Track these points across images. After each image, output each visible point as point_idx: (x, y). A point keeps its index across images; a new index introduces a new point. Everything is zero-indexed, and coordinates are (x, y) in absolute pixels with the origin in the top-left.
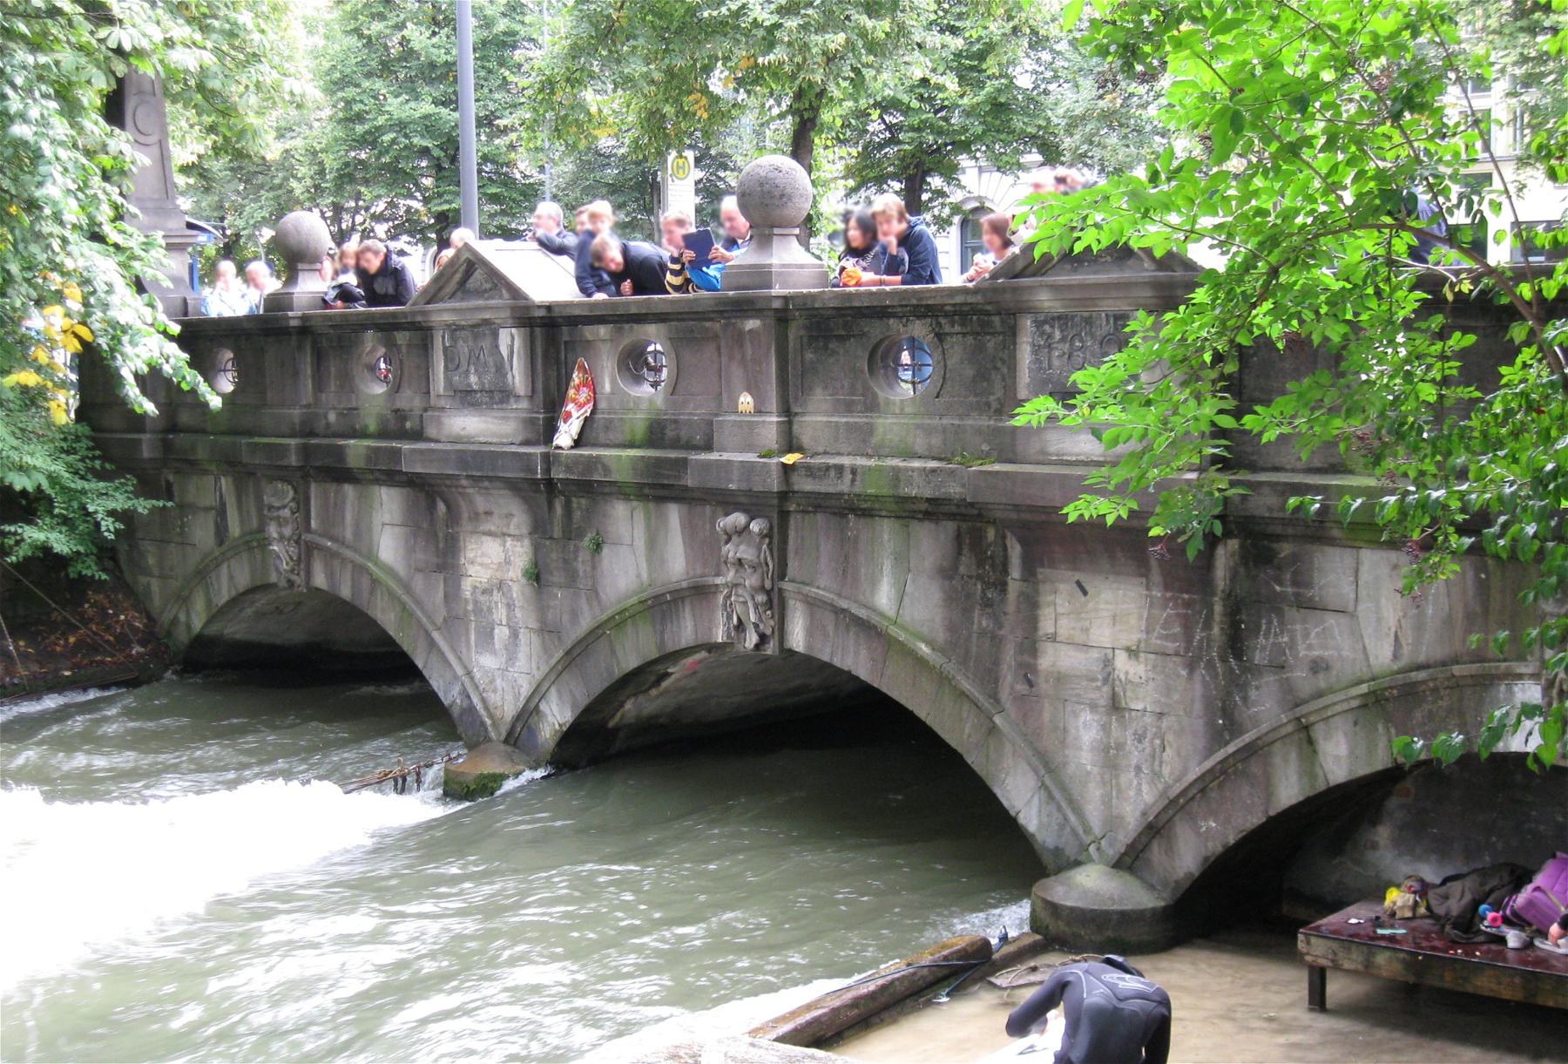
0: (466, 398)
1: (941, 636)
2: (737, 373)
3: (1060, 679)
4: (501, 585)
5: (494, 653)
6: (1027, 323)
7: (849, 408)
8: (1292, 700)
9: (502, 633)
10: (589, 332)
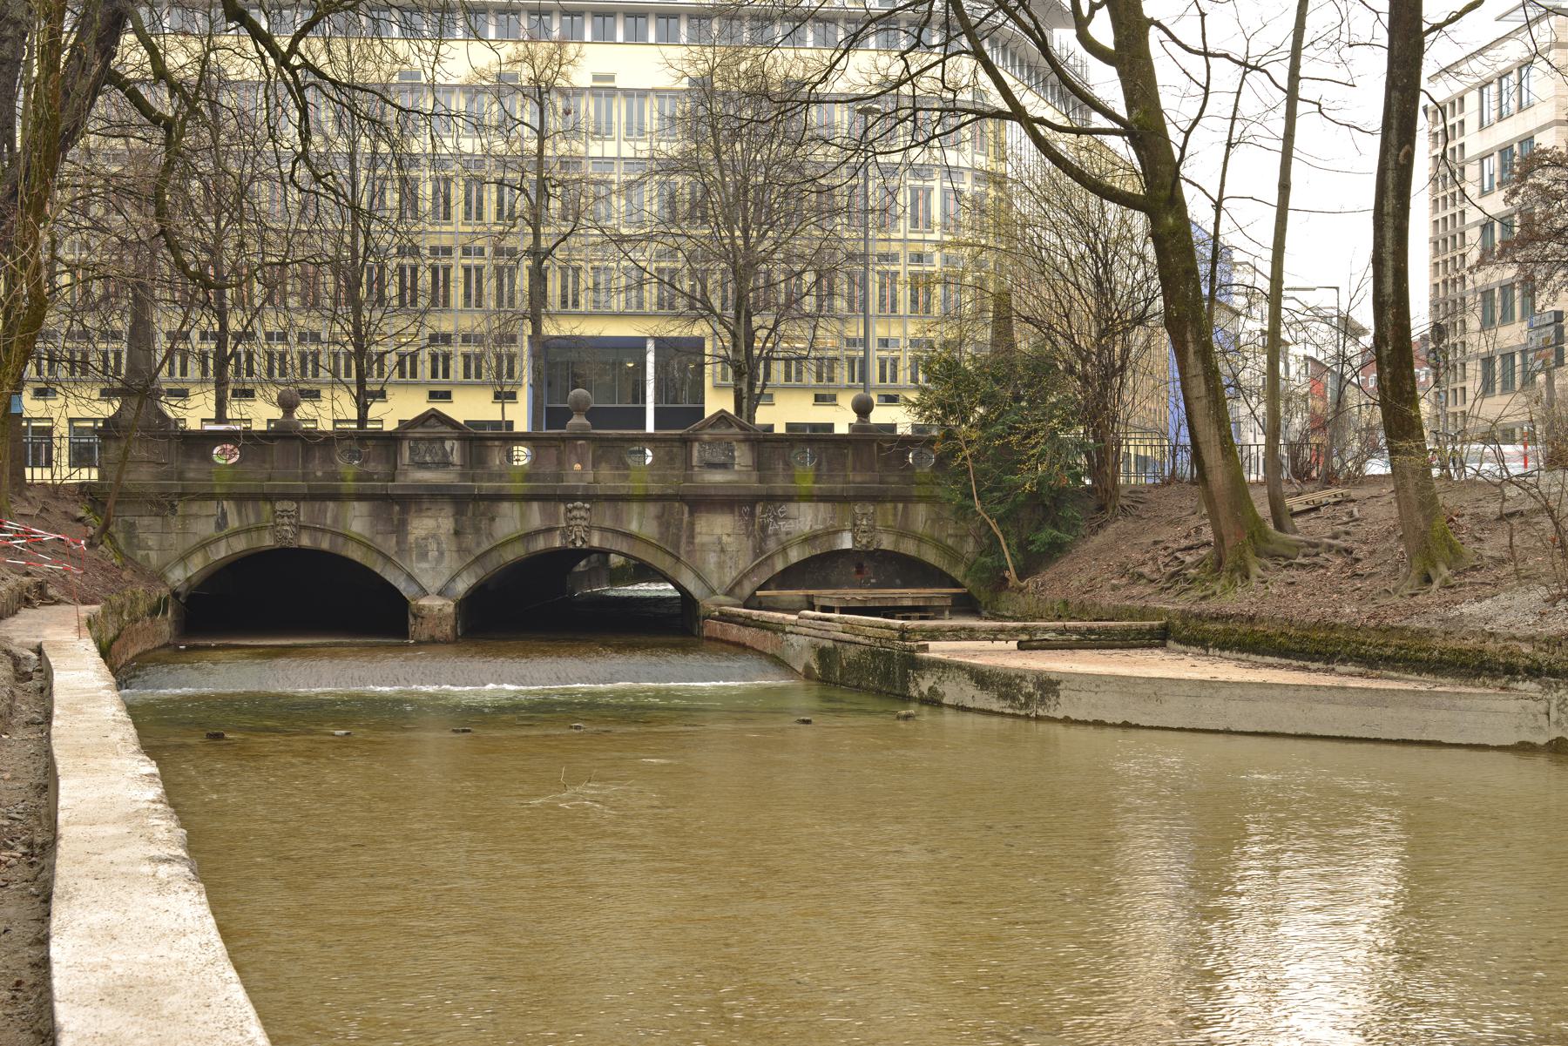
0: (423, 465)
1: (657, 537)
2: (573, 458)
3: (703, 545)
4: (434, 536)
5: (428, 561)
6: (696, 445)
7: (617, 469)
8: (780, 542)
9: (433, 554)
10: (489, 443)
